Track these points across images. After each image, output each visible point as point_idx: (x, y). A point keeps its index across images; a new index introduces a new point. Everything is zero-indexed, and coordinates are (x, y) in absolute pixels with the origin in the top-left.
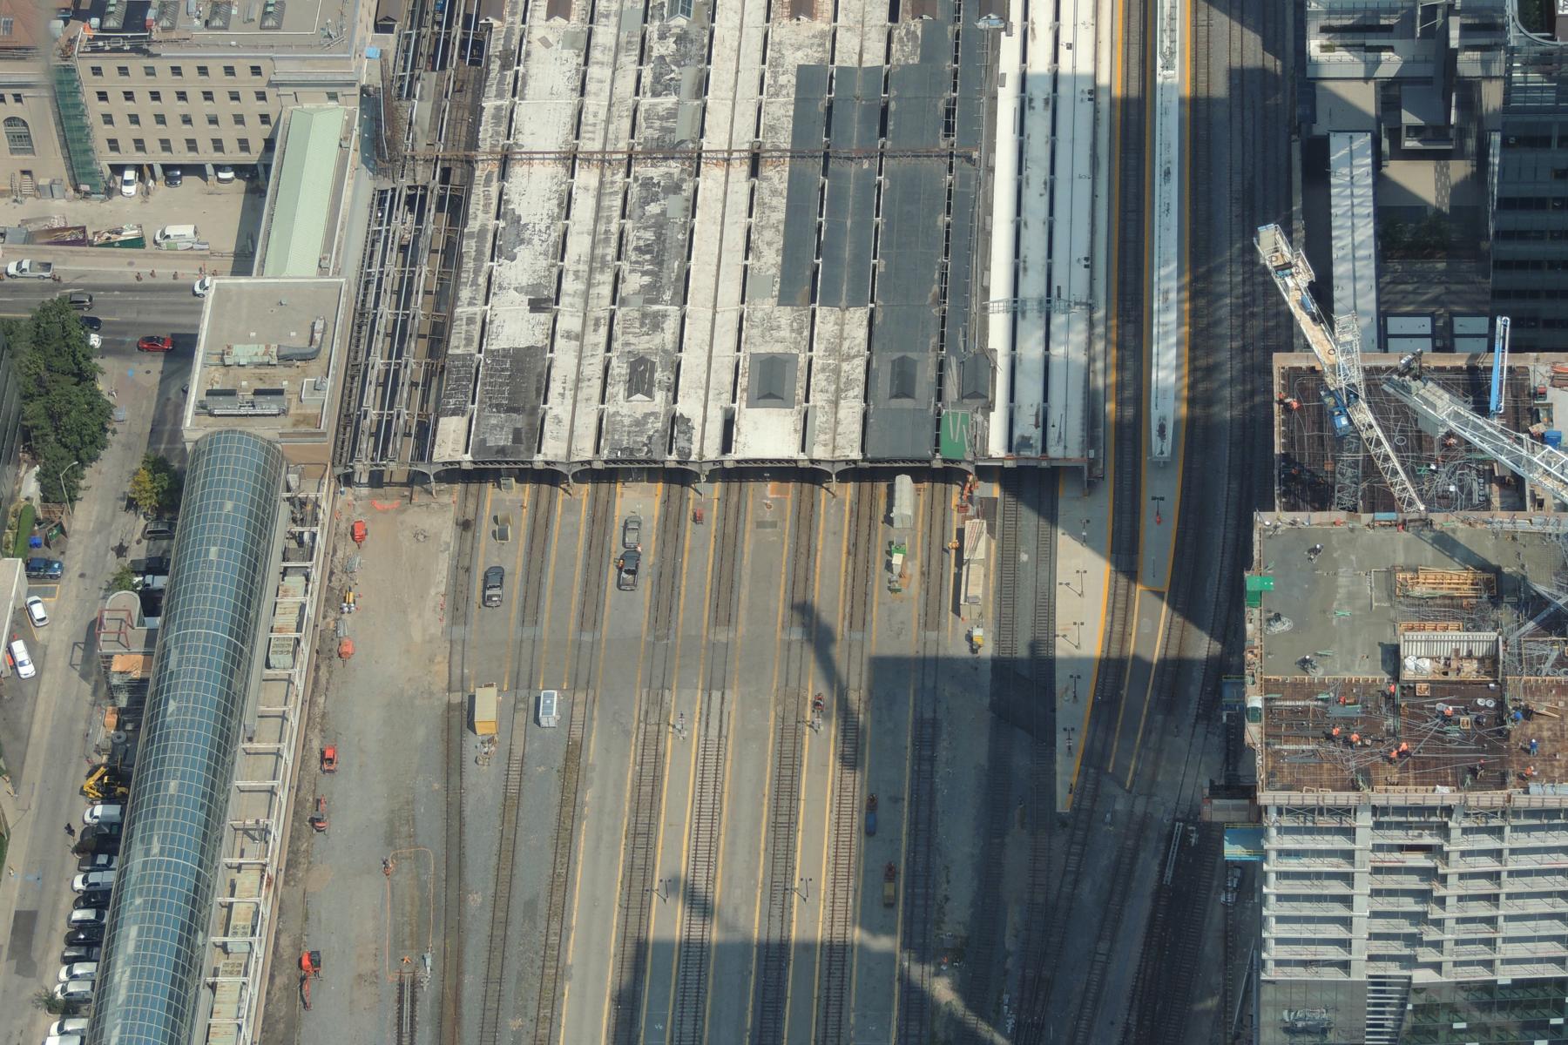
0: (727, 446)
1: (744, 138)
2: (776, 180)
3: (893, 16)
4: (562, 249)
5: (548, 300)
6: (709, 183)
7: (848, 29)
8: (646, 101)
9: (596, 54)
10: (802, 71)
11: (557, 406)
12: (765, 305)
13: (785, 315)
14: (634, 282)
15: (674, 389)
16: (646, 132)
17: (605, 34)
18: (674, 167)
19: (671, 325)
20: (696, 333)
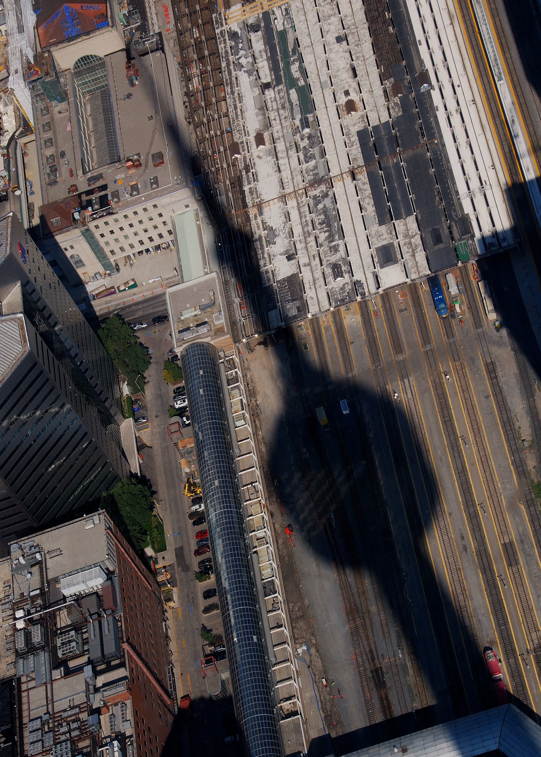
1: (346, 166)
2: (363, 179)
4: (291, 233)
5: (293, 254)
6: (338, 188)
7: (371, 111)
9: (279, 155)
10: (359, 133)
11: (309, 294)
12: (375, 228)
13: (383, 229)
14: (323, 237)
17: (281, 146)
18: (323, 187)
19: (342, 248)
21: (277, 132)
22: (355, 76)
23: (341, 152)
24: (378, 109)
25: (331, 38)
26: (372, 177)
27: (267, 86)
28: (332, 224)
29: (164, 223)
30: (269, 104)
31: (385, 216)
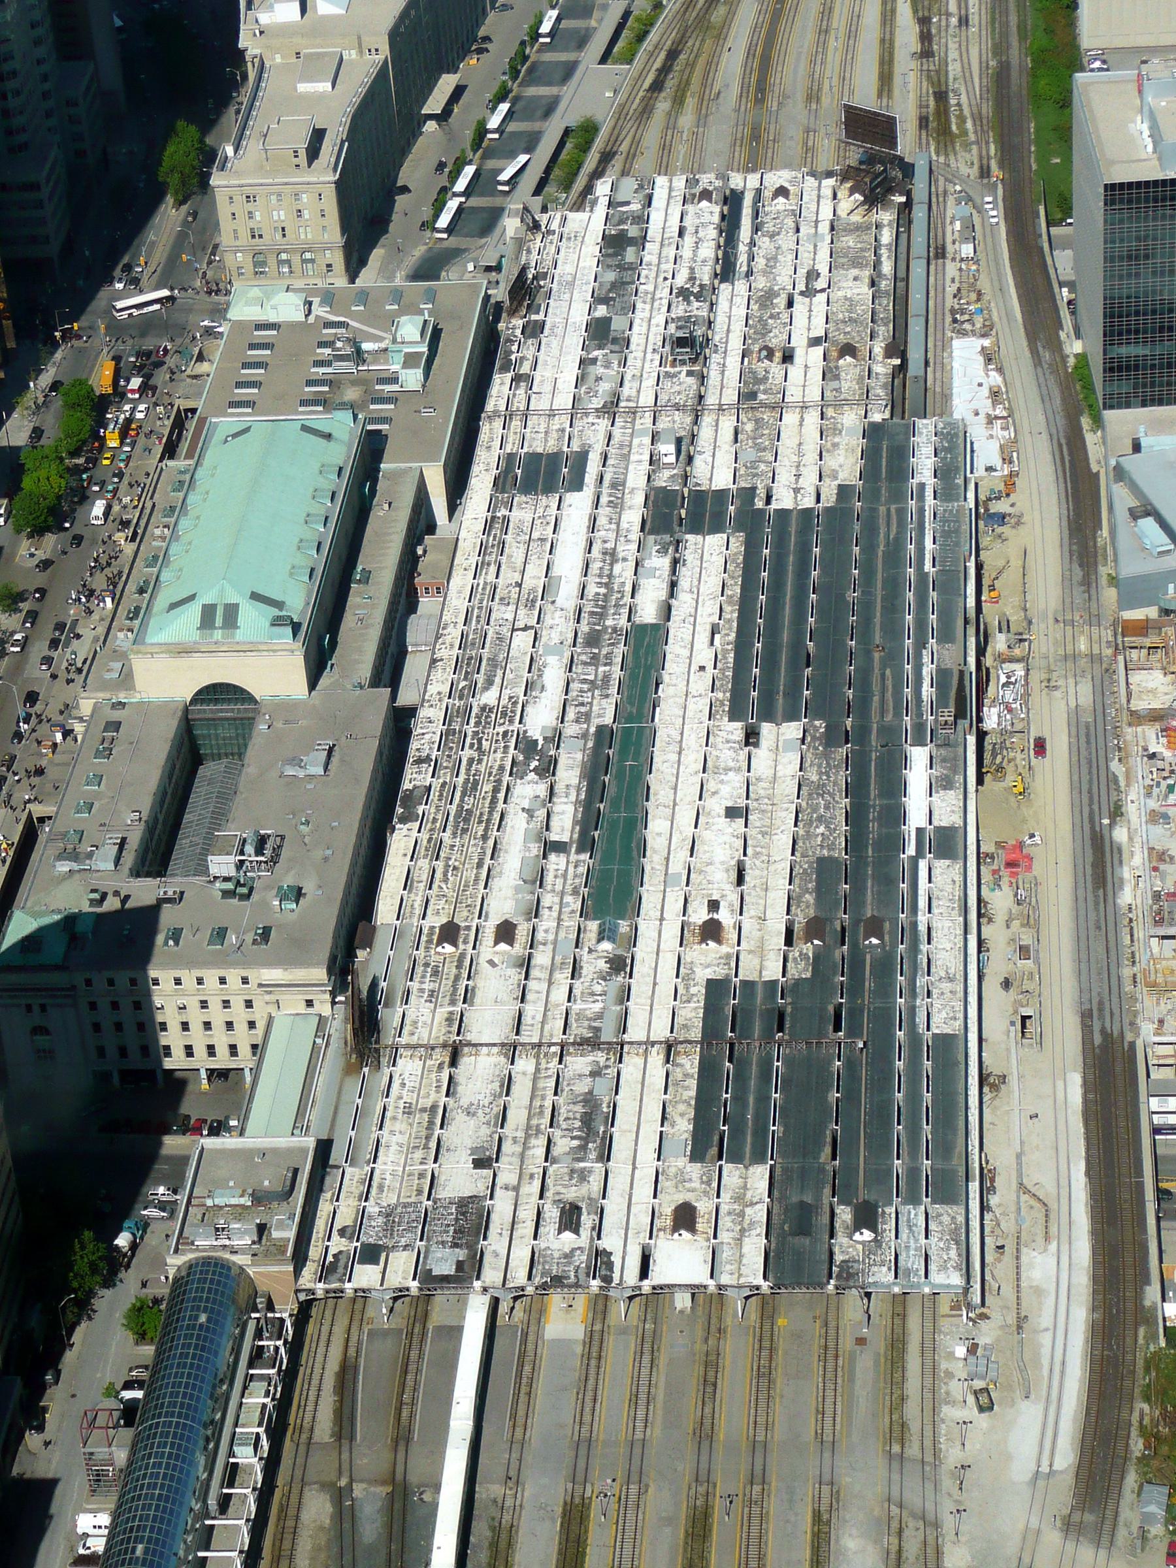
0: (644, 1273)
1: (661, 1031)
2: (688, 1066)
3: (789, 941)
5: (490, 1159)
6: (631, 1069)
7: (750, 952)
8: (576, 1007)
9: (534, 973)
10: (710, 983)
11: (495, 1244)
12: (678, 1162)
15: (598, 1230)
16: (579, 1030)
17: (542, 958)
18: (600, 1057)
20: (618, 1184)
21: (546, 931)
22: (740, 880)
23: (663, 1000)
24: (764, 951)
25: (716, 806)
26: (708, 1072)
27: (559, 847)
28: (595, 1128)
29: (252, 1025)
30: (549, 878)
31: (709, 1143)
